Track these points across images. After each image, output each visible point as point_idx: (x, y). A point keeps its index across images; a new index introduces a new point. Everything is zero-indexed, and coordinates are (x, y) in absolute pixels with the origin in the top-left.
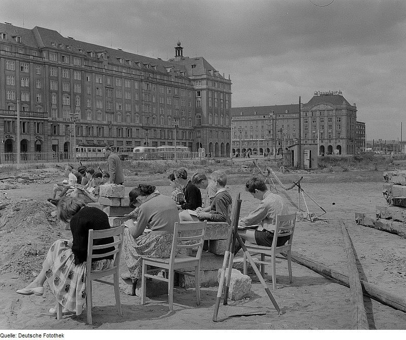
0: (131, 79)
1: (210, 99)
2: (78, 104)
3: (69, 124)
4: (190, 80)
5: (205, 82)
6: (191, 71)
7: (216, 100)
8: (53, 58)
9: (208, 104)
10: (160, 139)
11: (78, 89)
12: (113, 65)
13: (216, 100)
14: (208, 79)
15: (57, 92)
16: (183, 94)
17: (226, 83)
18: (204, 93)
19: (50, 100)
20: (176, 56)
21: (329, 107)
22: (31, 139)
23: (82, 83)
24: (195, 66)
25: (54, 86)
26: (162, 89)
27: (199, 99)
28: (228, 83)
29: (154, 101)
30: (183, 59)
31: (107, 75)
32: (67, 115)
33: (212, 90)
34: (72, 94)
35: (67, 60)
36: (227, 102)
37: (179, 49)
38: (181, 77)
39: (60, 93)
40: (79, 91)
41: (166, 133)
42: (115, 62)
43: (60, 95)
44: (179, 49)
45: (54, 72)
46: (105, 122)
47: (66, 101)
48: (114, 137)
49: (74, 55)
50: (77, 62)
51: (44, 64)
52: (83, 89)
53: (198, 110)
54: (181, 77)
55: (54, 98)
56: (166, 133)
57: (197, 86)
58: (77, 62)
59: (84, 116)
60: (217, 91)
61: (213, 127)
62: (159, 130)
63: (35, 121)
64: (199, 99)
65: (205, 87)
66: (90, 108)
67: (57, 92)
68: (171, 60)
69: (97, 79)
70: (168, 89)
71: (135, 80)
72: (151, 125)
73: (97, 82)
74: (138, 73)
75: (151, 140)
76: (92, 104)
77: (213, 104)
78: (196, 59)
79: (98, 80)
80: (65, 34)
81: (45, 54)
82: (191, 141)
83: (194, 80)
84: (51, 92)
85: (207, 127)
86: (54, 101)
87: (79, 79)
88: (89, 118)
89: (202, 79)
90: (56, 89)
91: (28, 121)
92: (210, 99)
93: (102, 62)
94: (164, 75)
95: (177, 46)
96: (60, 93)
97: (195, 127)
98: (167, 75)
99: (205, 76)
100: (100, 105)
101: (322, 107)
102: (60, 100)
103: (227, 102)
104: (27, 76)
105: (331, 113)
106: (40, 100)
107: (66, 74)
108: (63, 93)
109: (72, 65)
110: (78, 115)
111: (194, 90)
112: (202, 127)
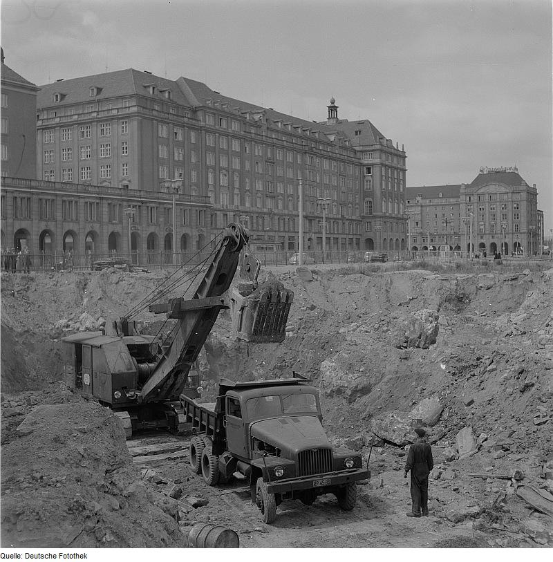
0: (292, 150)
1: (384, 178)
2: (237, 185)
3: (228, 213)
4: (355, 152)
5: (377, 154)
6: (355, 140)
7: (390, 180)
8: (210, 121)
9: (381, 185)
10: (279, 231)
11: (236, 164)
12: (273, 130)
13: (390, 180)
14: (381, 151)
15: (227, 170)
16: (350, 170)
17: (400, 156)
18: (376, 171)
19: (207, 178)
20: (329, 118)
21: (503, 189)
22: (193, 233)
23: (241, 155)
24: (360, 132)
25: (210, 160)
26: (326, 164)
27: (370, 178)
28: (402, 156)
29: (318, 181)
30: (339, 122)
31: (268, 145)
32: (224, 200)
33: (385, 166)
34: (230, 170)
35: (224, 123)
36: (402, 182)
37: (333, 108)
38: (345, 148)
39: (216, 169)
40: (238, 167)
41: (332, 225)
42: (273, 126)
43: (217, 172)
44: (333, 108)
45: (210, 140)
46: (265, 210)
47: (224, 181)
48: (275, 231)
49: (231, 117)
50: (235, 127)
51: (201, 128)
52: (242, 164)
53: (369, 193)
54: (345, 148)
55: (210, 176)
56: (332, 225)
57: (367, 160)
58: (235, 127)
59: (242, 202)
60: (392, 167)
61: (387, 217)
62: (232, 213)
63: (197, 208)
64: (370, 178)
65: (378, 161)
66: (249, 191)
67: (214, 168)
68: (323, 124)
69: (256, 151)
70: (334, 164)
71: (298, 152)
72: (316, 215)
73: (257, 154)
74: (299, 141)
75: (316, 235)
76: (251, 185)
77: (387, 185)
78: (360, 123)
79: (258, 151)
80: (213, 88)
81: (200, 115)
82: (358, 237)
83: (362, 152)
84: (208, 167)
85: (381, 217)
86: (211, 181)
87: (238, 149)
88: (248, 205)
89: (373, 150)
90: (212, 163)
91: (98, 201)
92: (384, 178)
93: (260, 127)
94: (328, 145)
95: (330, 104)
96: (216, 169)
97: (363, 218)
98: (331, 144)
99: (378, 147)
100: (259, 186)
101: (492, 188)
102: (217, 180)
103: (402, 182)
104: (181, 145)
105: (505, 197)
106: (194, 179)
107: (223, 143)
108: (221, 169)
109: (230, 131)
110: (237, 201)
111: (362, 165)
112: (374, 217)
